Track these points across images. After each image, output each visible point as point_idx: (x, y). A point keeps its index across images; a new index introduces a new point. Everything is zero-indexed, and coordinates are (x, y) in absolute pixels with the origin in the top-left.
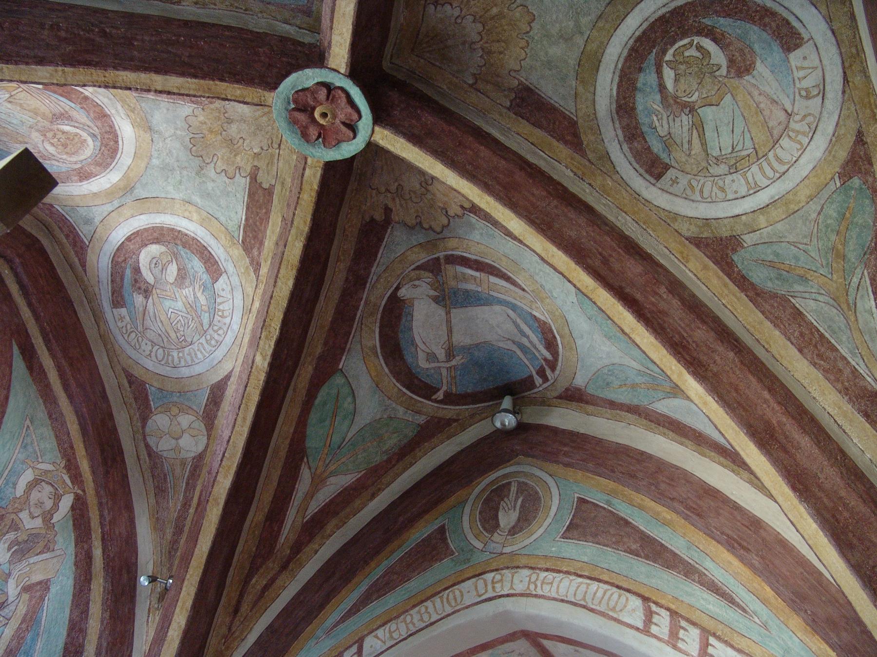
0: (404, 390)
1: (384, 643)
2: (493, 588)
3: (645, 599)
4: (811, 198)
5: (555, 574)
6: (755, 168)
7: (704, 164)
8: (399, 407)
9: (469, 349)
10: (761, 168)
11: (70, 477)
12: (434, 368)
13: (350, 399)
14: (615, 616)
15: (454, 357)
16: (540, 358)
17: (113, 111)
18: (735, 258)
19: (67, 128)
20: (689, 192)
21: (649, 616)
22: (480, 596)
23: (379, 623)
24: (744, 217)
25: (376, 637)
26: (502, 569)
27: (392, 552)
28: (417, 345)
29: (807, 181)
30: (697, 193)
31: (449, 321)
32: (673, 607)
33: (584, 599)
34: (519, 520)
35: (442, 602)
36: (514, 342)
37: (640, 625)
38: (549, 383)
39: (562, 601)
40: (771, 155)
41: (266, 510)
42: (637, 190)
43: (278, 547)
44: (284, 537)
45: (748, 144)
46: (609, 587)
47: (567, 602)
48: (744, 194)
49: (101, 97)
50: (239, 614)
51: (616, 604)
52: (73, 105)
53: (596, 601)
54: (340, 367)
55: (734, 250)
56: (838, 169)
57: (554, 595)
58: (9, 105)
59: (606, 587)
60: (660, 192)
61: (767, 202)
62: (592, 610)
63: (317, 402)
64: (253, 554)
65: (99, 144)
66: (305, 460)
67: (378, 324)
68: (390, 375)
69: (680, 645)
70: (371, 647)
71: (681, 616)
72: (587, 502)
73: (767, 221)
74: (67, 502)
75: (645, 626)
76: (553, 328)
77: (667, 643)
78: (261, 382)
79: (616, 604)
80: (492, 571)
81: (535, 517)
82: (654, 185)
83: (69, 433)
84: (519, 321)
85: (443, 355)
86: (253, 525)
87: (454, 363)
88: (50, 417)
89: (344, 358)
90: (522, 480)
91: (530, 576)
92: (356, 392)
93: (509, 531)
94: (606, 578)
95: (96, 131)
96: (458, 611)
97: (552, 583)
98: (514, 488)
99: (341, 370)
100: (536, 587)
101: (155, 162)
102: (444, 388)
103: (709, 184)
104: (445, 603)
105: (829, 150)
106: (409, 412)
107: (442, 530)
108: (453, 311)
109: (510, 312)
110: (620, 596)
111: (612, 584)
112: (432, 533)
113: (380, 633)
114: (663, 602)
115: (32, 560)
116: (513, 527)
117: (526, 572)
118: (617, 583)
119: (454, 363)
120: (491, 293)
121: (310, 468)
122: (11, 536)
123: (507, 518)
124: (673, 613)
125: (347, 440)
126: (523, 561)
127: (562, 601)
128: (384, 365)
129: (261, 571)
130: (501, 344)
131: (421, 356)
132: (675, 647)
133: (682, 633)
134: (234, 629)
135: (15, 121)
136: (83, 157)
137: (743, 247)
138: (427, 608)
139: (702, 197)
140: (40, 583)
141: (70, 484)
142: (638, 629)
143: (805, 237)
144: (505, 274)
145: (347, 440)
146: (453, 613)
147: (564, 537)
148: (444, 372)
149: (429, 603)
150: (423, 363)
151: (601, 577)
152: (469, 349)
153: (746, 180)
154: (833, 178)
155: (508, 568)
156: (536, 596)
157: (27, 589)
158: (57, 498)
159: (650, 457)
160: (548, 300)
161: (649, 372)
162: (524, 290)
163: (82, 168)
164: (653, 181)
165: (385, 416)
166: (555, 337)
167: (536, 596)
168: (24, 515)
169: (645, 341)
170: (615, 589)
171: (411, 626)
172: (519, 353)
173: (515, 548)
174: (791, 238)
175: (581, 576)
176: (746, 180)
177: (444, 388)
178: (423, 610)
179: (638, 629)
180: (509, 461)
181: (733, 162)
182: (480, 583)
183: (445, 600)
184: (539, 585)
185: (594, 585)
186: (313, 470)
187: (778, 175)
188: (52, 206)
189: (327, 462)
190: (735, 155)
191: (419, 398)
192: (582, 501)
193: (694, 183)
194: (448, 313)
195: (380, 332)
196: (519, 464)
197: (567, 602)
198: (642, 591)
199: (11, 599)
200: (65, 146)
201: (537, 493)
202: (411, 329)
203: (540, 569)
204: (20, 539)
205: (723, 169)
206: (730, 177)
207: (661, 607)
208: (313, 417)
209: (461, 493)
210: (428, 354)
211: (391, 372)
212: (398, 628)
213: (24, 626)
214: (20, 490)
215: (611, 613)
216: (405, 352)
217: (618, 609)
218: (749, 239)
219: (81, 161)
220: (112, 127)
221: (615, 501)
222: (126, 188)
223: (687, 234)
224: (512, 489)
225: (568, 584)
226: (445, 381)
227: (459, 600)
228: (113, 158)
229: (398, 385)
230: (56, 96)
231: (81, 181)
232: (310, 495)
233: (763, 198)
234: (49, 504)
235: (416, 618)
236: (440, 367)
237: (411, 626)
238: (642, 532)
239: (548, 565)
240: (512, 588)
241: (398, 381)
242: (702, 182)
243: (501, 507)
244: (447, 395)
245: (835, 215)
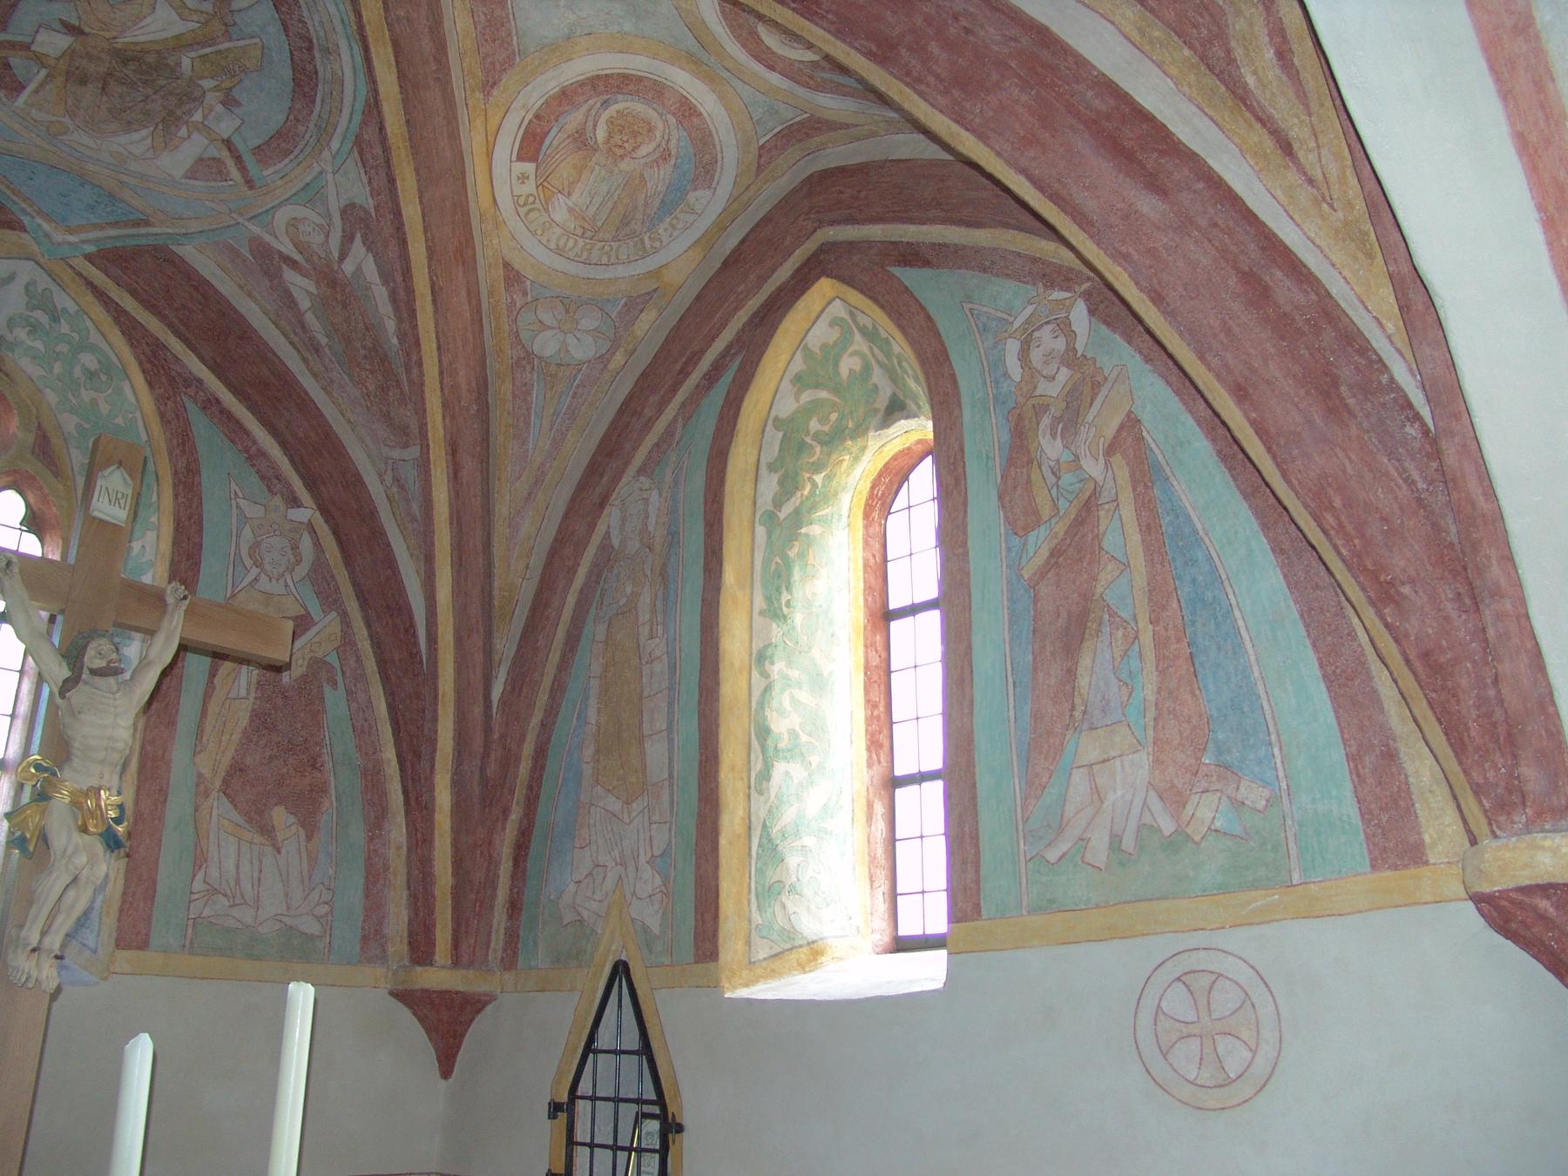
11: (1062, 289)
17: (553, 84)
19: (601, 134)
49: (533, 100)
50: (1296, 146)
52: (554, 131)
58: (574, 197)
64: (1195, 59)
65: (620, 97)
74: (1079, 314)
83: (1019, 254)
86: (1137, 38)
88: (985, 270)
95: (596, 101)
101: (628, 27)
115: (1090, 418)
122: (1046, 421)
129: (1238, 53)
134: (1317, 174)
135: (604, 188)
136: (655, 115)
140: (1121, 427)
141: (1067, 295)
157: (1111, 450)
158: (1065, 327)
163: (674, 114)
168: (1043, 387)
188: (762, 147)
199: (1099, 478)
200: (635, 134)
204: (1058, 414)
213: (1140, 488)
214: (1015, 371)
219: (661, 115)
220: (582, 84)
222: (694, 63)
228: (640, 79)
230: (544, 148)
231: (700, 114)
234: (1060, 344)
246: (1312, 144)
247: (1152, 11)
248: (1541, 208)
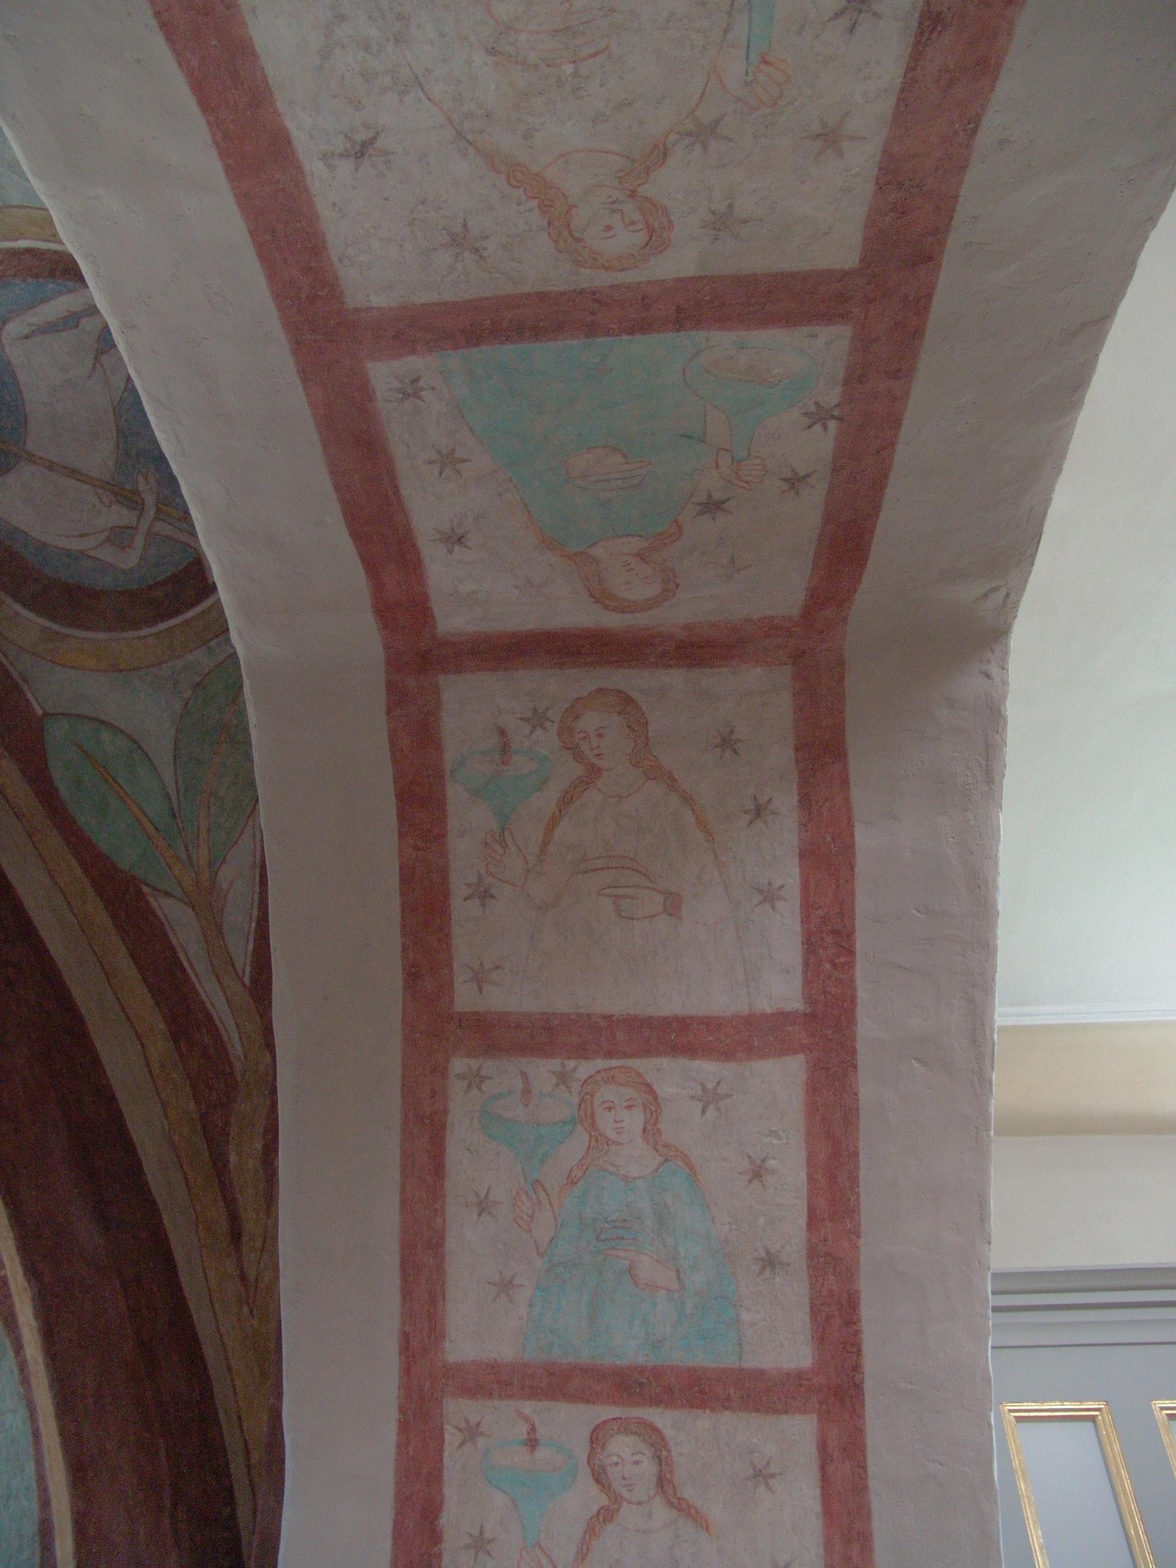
0: (163, 626)
8: (191, 657)
9: (127, 454)
13: (105, 735)
15: (135, 492)
28: (82, 552)
31: (51, 466)
41: (162, 1026)
43: (237, 1064)
44: (236, 1040)
50: (245, 1238)
54: (40, 712)
63: (64, 791)
64: (196, 1116)
66: (146, 889)
67: (9, 600)
68: (116, 635)
85: (125, 511)
87: (150, 500)
89: (30, 696)
92: (102, 716)
99: (46, 714)
106: (213, 643)
108: (30, 446)
119: (150, 500)
121: (168, 894)
125: (172, 792)
129: (234, 1130)
131: (107, 554)
134: (252, 1274)
145: (172, 792)
150: (129, 560)
152: (127, 454)
186: (178, 892)
189: (184, 856)
191: (198, 609)
194: (31, 459)
208: (85, 818)
210: (108, 539)
211: (109, 629)
229: (146, 631)
232: (213, 931)
241: (135, 626)
246: (259, 1244)
247: (181, 1054)
248: (402, 1409)
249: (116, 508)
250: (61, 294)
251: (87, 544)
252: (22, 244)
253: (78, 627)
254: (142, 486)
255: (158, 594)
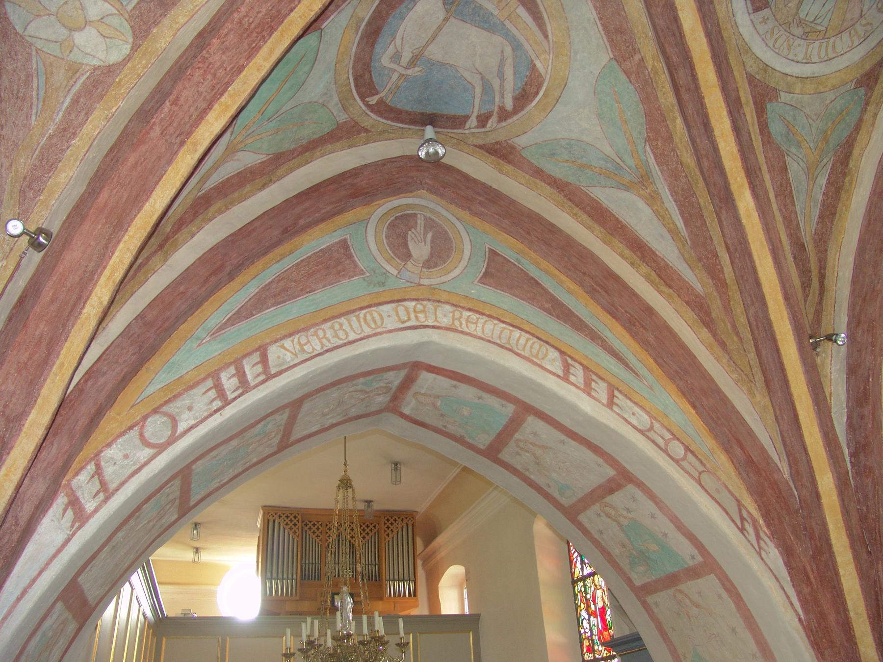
1: (296, 355)
2: (416, 317)
3: (562, 353)
4: (834, 88)
5: (478, 316)
6: (817, 44)
7: (790, 19)
10: (820, 47)
12: (390, 69)
13: (307, 68)
14: (539, 362)
15: (415, 66)
16: (497, 104)
18: (768, 106)
20: (768, 35)
21: (567, 368)
22: (404, 322)
23: (283, 332)
24: (789, 78)
25: (283, 347)
26: (423, 300)
27: (283, 256)
28: (395, 38)
29: (838, 74)
30: (773, 40)
31: (440, 28)
32: (585, 363)
33: (508, 342)
34: (431, 254)
35: (359, 321)
36: (482, 78)
37: (561, 373)
38: (483, 130)
39: (489, 341)
40: (832, 40)
42: (735, 11)
45: (825, 23)
46: (531, 337)
47: (494, 343)
48: (799, 59)
51: (538, 352)
53: (520, 347)
54: (323, 27)
55: (771, 100)
56: (858, 76)
57: (480, 334)
59: (528, 336)
60: (749, 22)
61: (809, 75)
62: (518, 354)
68: (352, 58)
69: (593, 393)
70: (279, 357)
71: (593, 372)
72: (499, 255)
73: (801, 90)
75: (565, 374)
76: (545, 85)
77: (584, 391)
78: (313, 13)
79: (538, 352)
80: (412, 300)
81: (449, 257)
82: (749, 14)
84: (509, 62)
85: (408, 60)
87: (409, 72)
90: (429, 215)
91: (453, 312)
93: (424, 264)
94: (527, 329)
96: (380, 333)
97: (476, 323)
98: (420, 222)
100: (461, 324)
102: (382, 95)
103: (784, 37)
104: (363, 323)
105: (863, 60)
107: (344, 245)
108: (452, 20)
109: (508, 50)
110: (541, 346)
111: (533, 335)
112: (333, 245)
113: (287, 343)
114: (577, 357)
116: (427, 261)
117: (448, 308)
118: (536, 334)
119: (409, 72)
120: (507, 23)
123: (420, 249)
124: (585, 368)
126: (444, 297)
127: (489, 341)
128: (356, 45)
130: (466, 75)
131: (391, 50)
132: (589, 394)
133: (593, 385)
137: (777, 100)
138: (341, 325)
139: (774, 46)
142: (558, 376)
143: (815, 115)
144: (539, 12)
146: (375, 335)
147: (481, 281)
148: (395, 77)
149: (343, 320)
150: (385, 61)
151: (521, 326)
153: (807, 49)
154: (852, 81)
155: (429, 300)
156: (462, 332)
159: (560, 231)
160: (565, 58)
161: (618, 161)
162: (546, 37)
164: (751, 11)
165: (320, 101)
166: (537, 93)
167: (462, 332)
169: (728, 148)
170: (535, 340)
171: (324, 341)
172: (478, 90)
173: (433, 282)
174: (807, 111)
175: (503, 322)
176: (807, 49)
177: (382, 95)
178: (337, 327)
179: (558, 376)
180: (411, 192)
181: (808, 30)
182: (401, 309)
183: (362, 320)
184: (464, 322)
185: (517, 333)
187: (826, 58)
190: (813, 25)
192: (493, 253)
193: (776, 31)
194: (446, 20)
195: (377, 7)
196: (421, 197)
197: (494, 343)
198: (558, 345)
201: (446, 232)
202: (403, 18)
203: (463, 308)
205: (798, 31)
206: (798, 41)
207: (576, 361)
209: (360, 212)
210: (398, 51)
212: (309, 342)
215: (535, 360)
216: (380, 40)
217: (540, 355)
218: (784, 97)
221: (523, 261)
223: (749, 69)
224: (419, 221)
225: (492, 327)
226: (388, 88)
227: (379, 323)
229: (351, 71)
233: (807, 70)
235: (329, 334)
236: (395, 70)
237: (324, 341)
238: (551, 295)
239: (470, 306)
240: (436, 320)
241: (353, 68)
242: (781, 33)
243: (409, 239)
244: (381, 102)
245: (838, 108)
249: (411, 55)
250: (514, 85)
251: (398, 41)
252: (541, 93)
253: (361, 39)
254: (417, 69)
255: (367, 76)
